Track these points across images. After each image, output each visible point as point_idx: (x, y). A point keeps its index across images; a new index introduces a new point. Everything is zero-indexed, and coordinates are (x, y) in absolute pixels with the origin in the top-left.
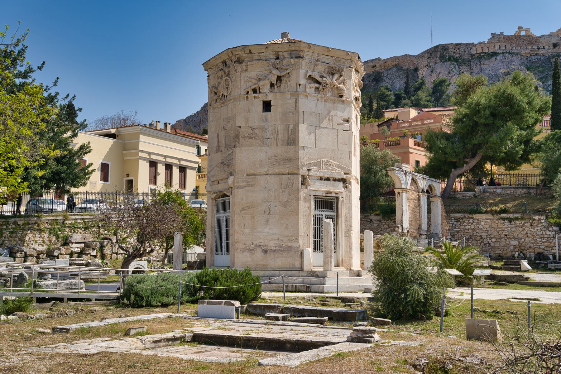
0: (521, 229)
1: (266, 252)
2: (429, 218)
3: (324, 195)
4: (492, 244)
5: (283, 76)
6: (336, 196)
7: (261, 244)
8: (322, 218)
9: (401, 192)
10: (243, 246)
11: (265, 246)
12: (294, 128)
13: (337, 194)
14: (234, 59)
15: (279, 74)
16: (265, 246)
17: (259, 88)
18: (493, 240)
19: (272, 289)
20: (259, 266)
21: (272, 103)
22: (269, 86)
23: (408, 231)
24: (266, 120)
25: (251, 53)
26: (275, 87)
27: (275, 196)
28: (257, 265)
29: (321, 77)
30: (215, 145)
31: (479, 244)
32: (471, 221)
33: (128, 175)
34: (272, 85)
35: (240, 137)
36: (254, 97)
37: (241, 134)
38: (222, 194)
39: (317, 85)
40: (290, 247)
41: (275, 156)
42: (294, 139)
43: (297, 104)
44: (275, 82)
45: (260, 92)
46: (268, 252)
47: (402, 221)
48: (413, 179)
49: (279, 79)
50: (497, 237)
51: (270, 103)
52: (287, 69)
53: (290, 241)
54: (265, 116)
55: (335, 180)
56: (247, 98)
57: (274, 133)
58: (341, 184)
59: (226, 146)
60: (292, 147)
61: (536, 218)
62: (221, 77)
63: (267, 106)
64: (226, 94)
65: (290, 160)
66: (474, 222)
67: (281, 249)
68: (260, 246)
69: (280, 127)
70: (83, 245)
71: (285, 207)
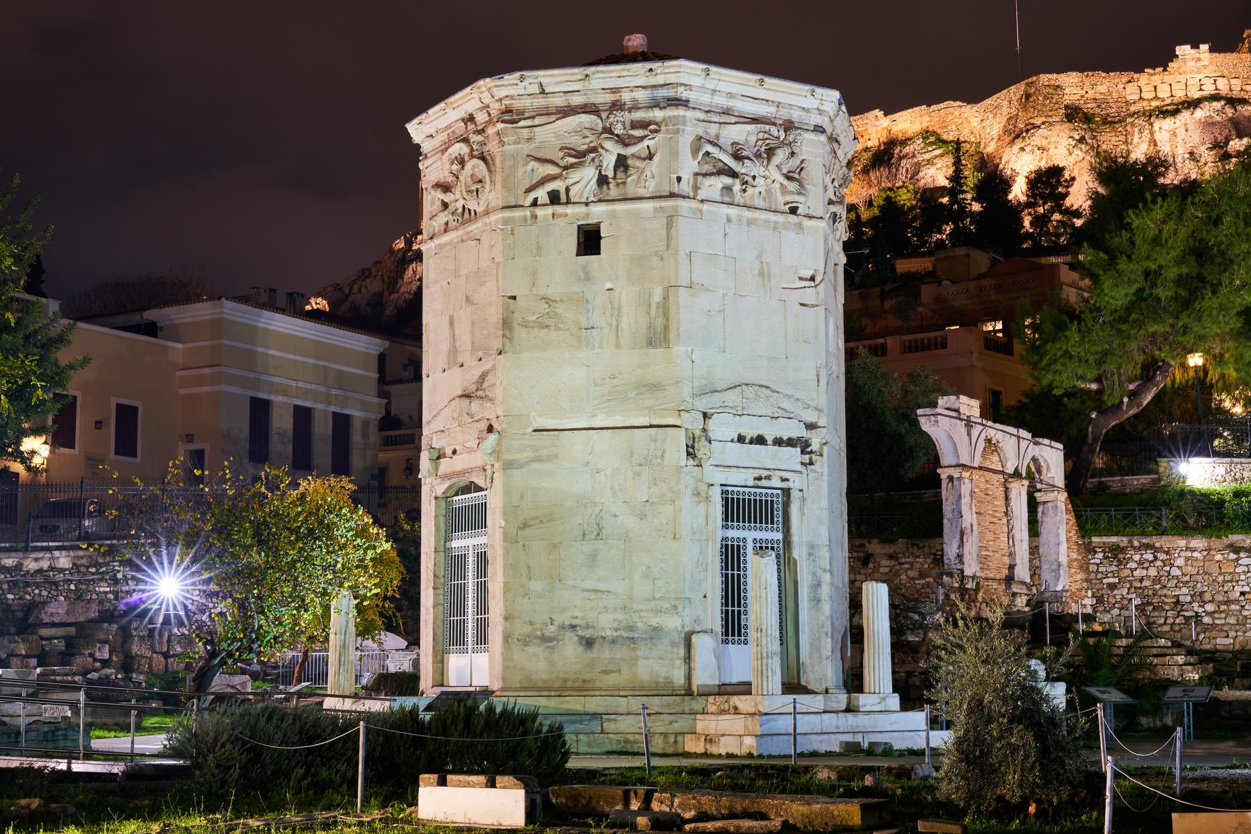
1: (589, 643)
2: (1034, 550)
3: (751, 483)
4: (1206, 620)
5: (633, 155)
6: (784, 485)
7: (575, 622)
8: (745, 547)
9: (956, 476)
10: (526, 629)
11: (588, 627)
12: (666, 298)
13: (784, 480)
14: (495, 108)
15: (623, 151)
16: (588, 627)
17: (568, 190)
18: (1210, 607)
19: (610, 749)
20: (570, 684)
22: (595, 180)
23: (978, 584)
24: (588, 277)
25: (543, 92)
26: (612, 186)
27: (612, 488)
28: (565, 680)
29: (737, 157)
30: (445, 347)
31: (1170, 621)
32: (1151, 557)
33: (190, 438)
34: (602, 181)
35: (515, 326)
36: (553, 215)
37: (518, 317)
38: (464, 481)
39: (727, 180)
40: (656, 629)
41: (613, 377)
42: (666, 328)
43: (673, 232)
44: (610, 174)
46: (597, 646)
47: (960, 557)
48: (988, 441)
49: (622, 163)
50: (1219, 598)
51: (599, 231)
52: (642, 138)
53: (658, 612)
54: (585, 268)
55: (778, 442)
56: (535, 217)
57: (608, 312)
59: (474, 349)
60: (658, 352)
62: (462, 162)
63: (590, 241)
64: (472, 205)
65: (655, 387)
66: (1156, 558)
67: (630, 634)
68: (573, 627)
69: (627, 295)
70: (72, 630)
71: (642, 517)
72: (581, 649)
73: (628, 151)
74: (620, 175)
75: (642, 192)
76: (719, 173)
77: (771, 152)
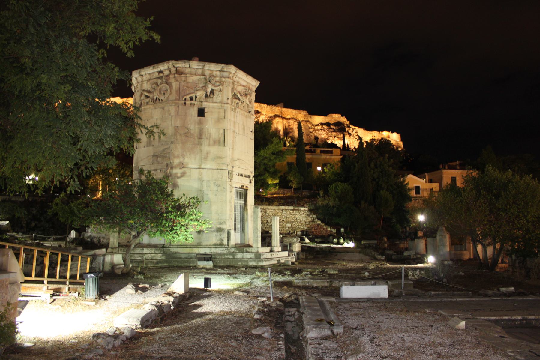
0: (293, 216)
13: (247, 187)
17: (196, 97)
21: (206, 110)
25: (190, 67)
29: (241, 95)
34: (206, 96)
39: (238, 101)
43: (226, 113)
44: (209, 94)
45: (196, 100)
56: (185, 103)
58: (248, 179)
60: (222, 147)
61: (302, 209)
63: (201, 113)
64: (162, 97)
72: (196, 234)
73: (214, 88)
74: (212, 96)
75: (218, 101)
76: (236, 98)
77: (246, 95)
